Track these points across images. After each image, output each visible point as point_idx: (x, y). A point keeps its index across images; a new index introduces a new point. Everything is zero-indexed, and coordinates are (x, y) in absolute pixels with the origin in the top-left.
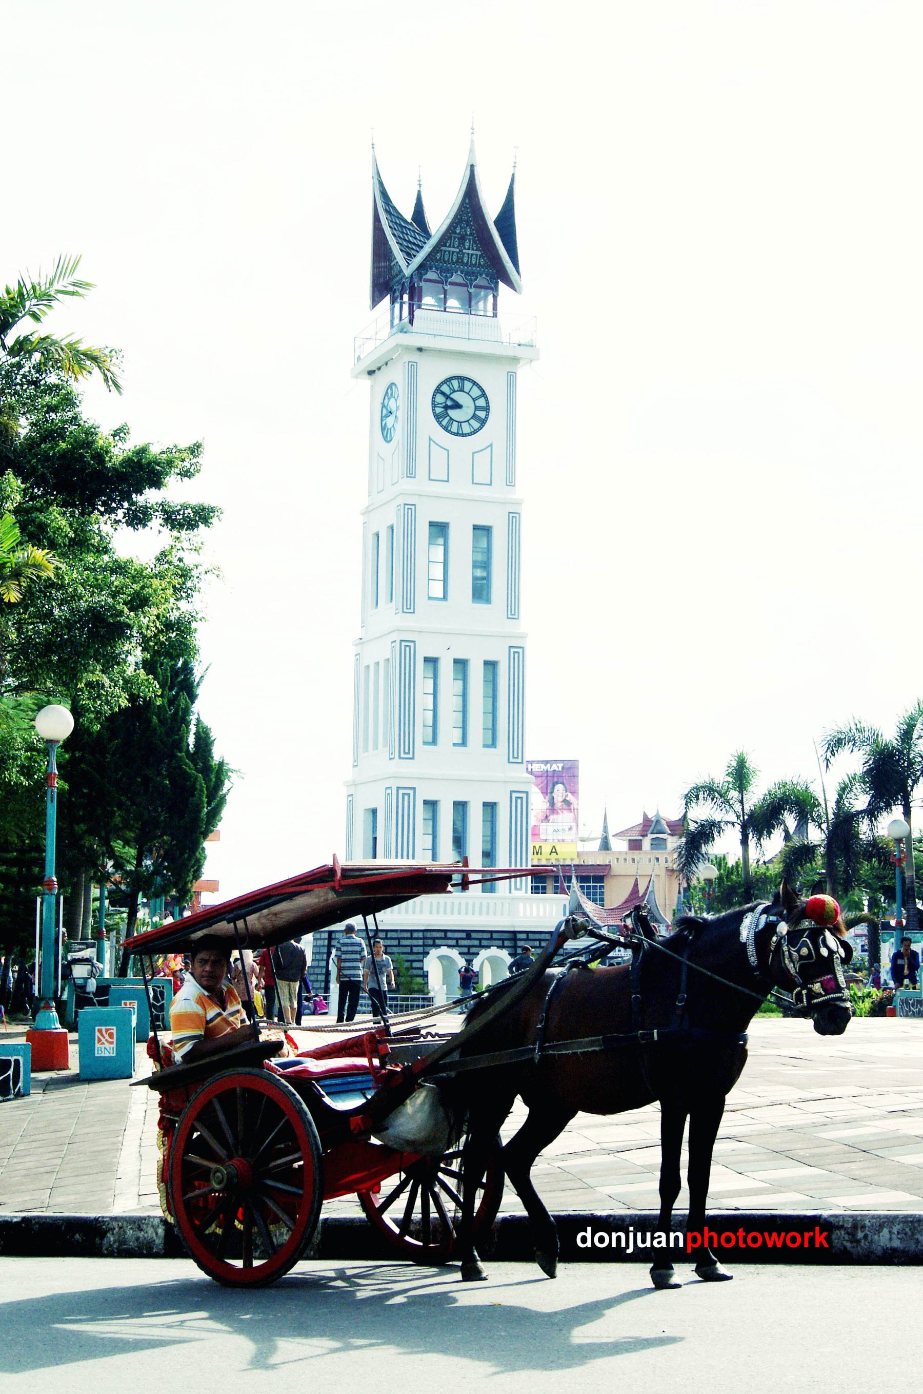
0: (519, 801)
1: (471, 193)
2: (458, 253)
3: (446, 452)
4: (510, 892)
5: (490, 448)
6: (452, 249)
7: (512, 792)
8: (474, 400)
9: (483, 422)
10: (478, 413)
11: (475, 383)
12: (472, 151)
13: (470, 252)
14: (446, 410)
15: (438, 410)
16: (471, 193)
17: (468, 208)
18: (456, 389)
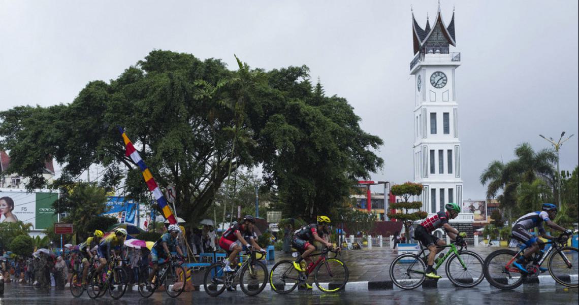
1: (439, 20)
9: (445, 84)
11: (442, 73)
12: (439, 8)
15: (432, 82)
16: (439, 20)
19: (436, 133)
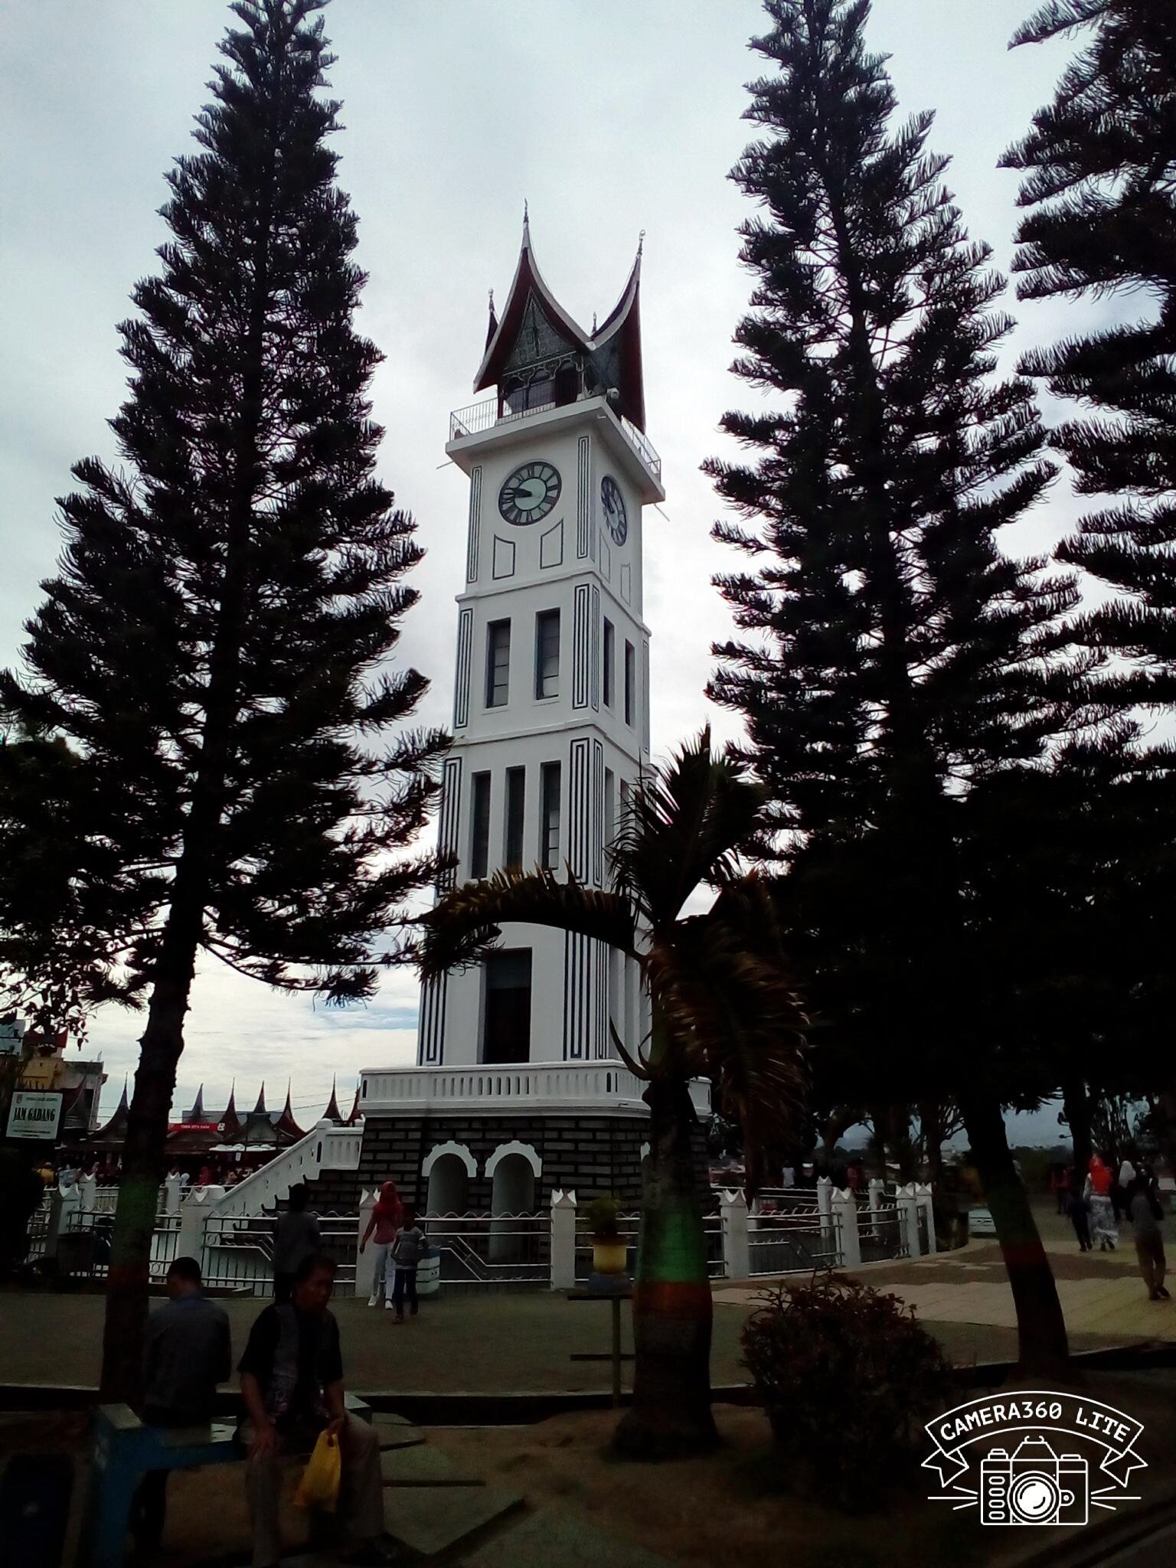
4: (565, 1059)
9: (553, 502)
10: (549, 494)
11: (545, 465)
15: (505, 507)
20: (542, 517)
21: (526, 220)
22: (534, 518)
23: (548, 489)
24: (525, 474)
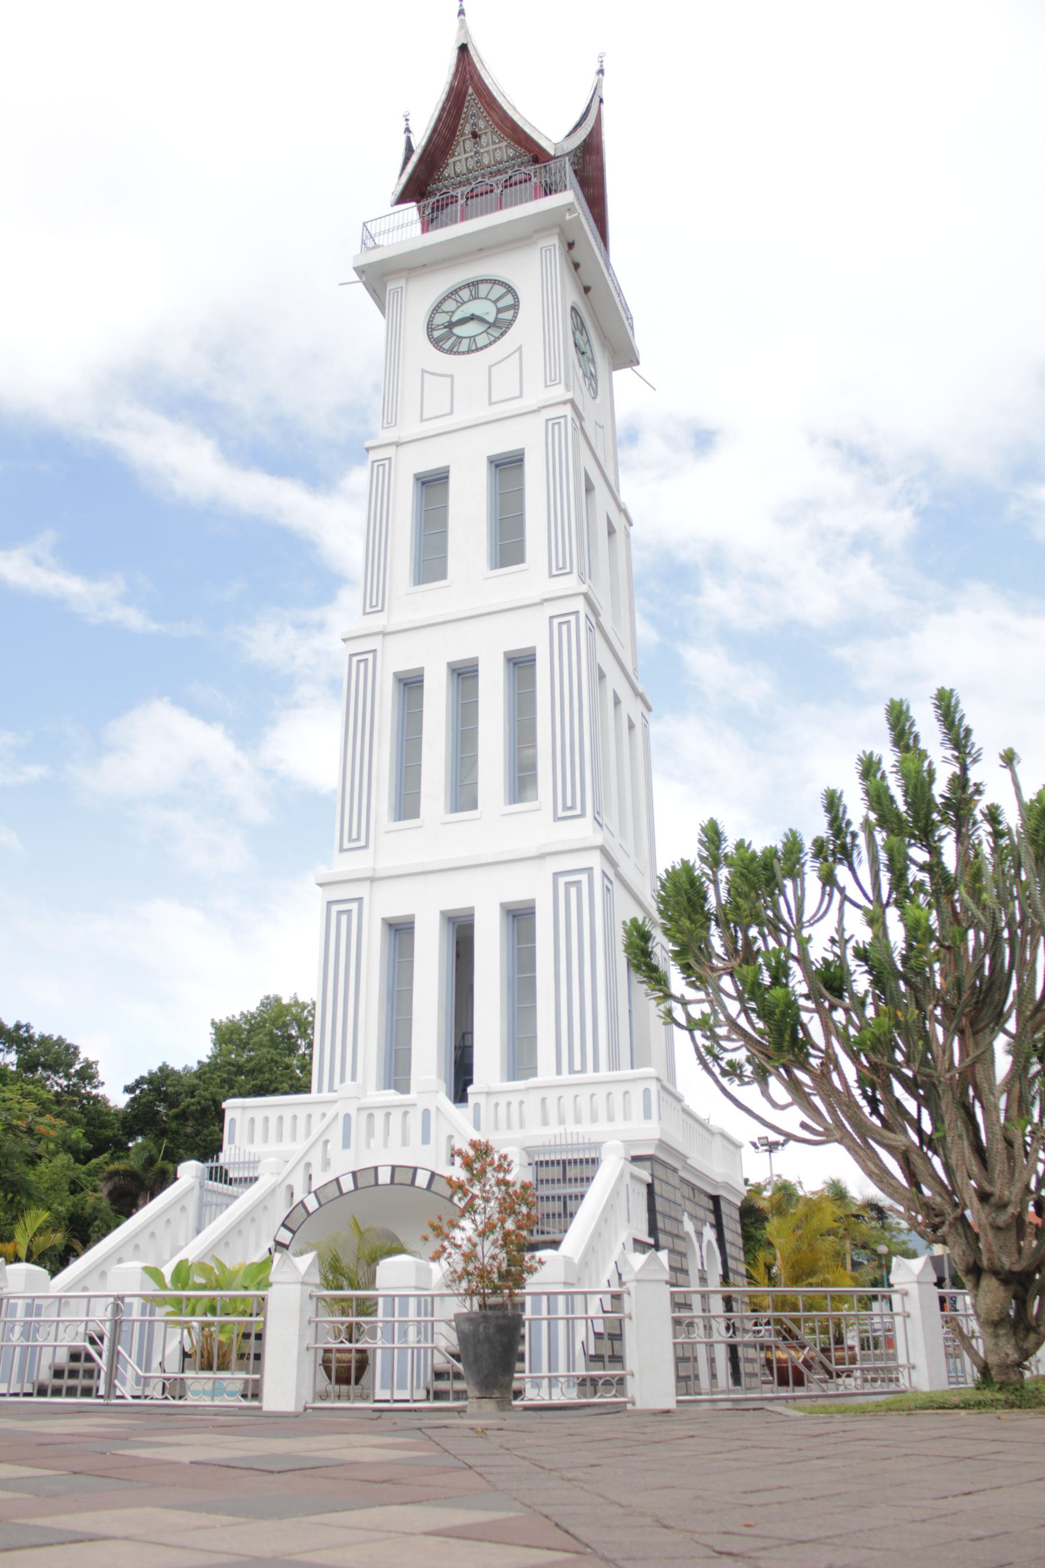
0: (573, 891)
2: (472, 157)
3: (449, 379)
5: (517, 355)
6: (463, 156)
7: (556, 875)
8: (495, 302)
10: (500, 316)
11: (495, 282)
13: (491, 147)
14: (451, 329)
15: (436, 334)
17: (474, 100)
18: (466, 299)
19: (440, 573)
20: (490, 344)
21: (461, 12)
22: (479, 346)
23: (499, 311)
24: (465, 294)
